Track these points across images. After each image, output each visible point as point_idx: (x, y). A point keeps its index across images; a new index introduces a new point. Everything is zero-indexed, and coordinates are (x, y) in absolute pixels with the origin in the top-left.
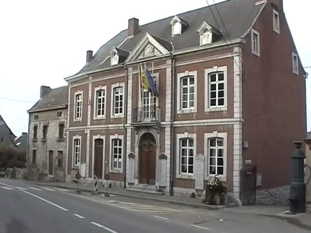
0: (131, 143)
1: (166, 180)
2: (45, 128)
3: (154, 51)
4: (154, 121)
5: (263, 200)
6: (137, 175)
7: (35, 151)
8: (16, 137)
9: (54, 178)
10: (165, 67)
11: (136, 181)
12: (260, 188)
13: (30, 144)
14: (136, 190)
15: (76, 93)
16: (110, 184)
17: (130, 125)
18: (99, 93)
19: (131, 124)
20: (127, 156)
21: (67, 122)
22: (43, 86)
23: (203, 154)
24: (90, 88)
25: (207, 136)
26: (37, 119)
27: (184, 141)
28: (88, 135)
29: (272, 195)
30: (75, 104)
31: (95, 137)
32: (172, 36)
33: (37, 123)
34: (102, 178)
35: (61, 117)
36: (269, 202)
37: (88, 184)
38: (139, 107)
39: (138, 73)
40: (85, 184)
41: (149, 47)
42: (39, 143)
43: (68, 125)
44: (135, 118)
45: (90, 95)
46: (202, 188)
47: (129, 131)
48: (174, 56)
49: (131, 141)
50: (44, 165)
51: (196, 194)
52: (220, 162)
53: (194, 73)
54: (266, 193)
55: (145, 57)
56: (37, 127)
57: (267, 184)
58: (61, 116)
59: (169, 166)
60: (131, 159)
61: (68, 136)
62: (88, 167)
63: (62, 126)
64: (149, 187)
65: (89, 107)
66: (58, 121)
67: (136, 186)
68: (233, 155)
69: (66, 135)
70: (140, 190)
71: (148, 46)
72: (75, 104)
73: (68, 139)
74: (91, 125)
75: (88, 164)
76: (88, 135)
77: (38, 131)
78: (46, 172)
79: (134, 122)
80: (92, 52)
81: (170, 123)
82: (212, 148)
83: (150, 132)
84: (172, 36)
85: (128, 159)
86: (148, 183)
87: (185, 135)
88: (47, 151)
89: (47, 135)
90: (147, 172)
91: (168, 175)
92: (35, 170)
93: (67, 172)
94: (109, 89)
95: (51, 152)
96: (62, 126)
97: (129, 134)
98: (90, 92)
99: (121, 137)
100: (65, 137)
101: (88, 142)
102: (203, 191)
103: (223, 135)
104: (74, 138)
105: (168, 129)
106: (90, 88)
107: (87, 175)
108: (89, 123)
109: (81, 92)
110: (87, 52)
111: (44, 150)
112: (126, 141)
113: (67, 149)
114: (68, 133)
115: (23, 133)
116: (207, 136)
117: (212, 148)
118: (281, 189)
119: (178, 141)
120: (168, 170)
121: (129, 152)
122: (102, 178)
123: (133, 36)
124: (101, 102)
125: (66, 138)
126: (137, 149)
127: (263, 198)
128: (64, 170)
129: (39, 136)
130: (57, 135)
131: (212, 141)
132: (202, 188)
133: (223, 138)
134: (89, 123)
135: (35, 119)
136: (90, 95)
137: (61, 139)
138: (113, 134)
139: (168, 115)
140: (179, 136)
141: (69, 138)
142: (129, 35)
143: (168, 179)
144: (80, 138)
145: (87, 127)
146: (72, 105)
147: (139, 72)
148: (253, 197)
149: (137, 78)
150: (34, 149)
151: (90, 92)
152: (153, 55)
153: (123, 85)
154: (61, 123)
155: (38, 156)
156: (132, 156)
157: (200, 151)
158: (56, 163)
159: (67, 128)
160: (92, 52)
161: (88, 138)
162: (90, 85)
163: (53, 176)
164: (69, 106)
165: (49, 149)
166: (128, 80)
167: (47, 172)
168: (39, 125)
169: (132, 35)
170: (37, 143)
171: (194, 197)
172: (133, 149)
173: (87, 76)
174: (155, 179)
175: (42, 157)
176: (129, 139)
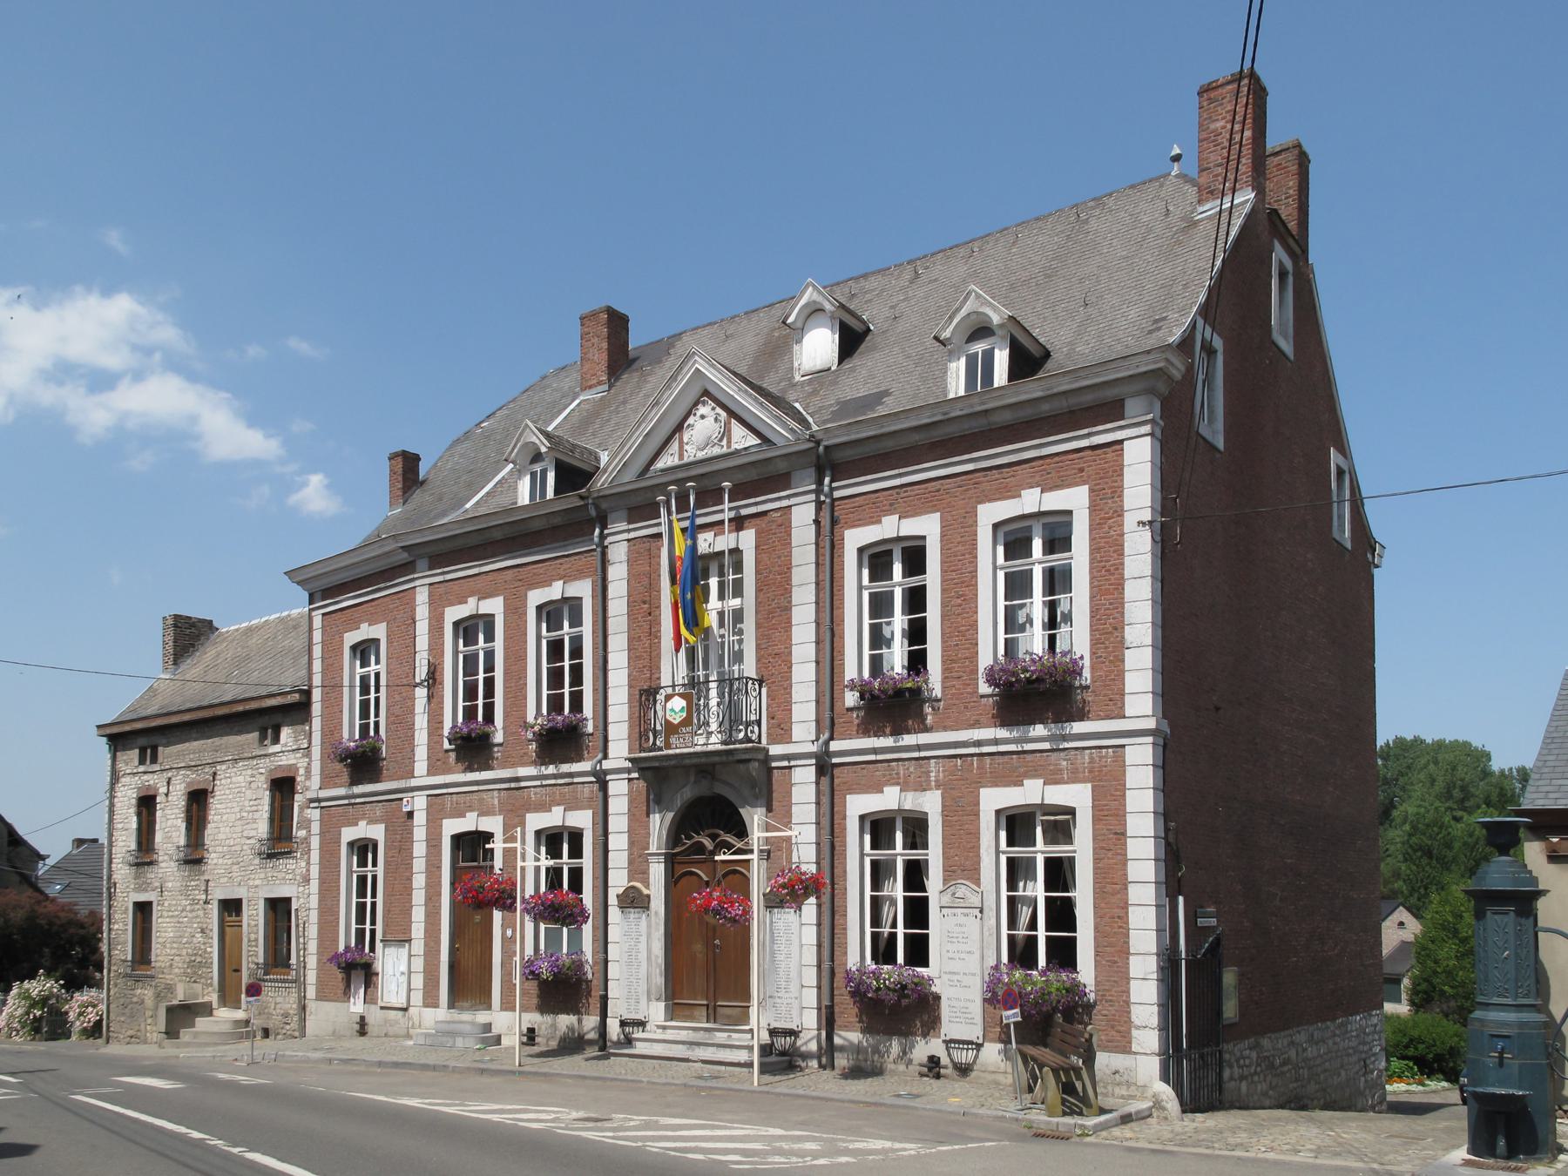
0: (631, 843)
1: (799, 998)
2: (198, 800)
3: (726, 433)
4: (741, 742)
5: (1244, 1086)
6: (659, 981)
7: (143, 910)
8: (43, 858)
9: (247, 1022)
10: (785, 503)
11: (656, 1012)
12: (1237, 1031)
13: (116, 877)
14: (658, 1050)
15: (352, 638)
16: (531, 1031)
17: (628, 764)
18: (468, 629)
19: (630, 760)
20: (613, 900)
21: (308, 770)
22: (177, 617)
23: (978, 882)
24: (422, 612)
25: (994, 799)
26: (154, 760)
27: (879, 828)
28: (420, 818)
29: (1272, 1066)
30: (346, 682)
31: (453, 826)
32: (798, 378)
33: (151, 780)
34: (489, 1007)
35: (277, 748)
36: (1265, 1094)
37: (427, 1035)
38: (665, 680)
39: (659, 535)
40: (408, 1036)
41: (703, 417)
42: (167, 866)
43: (316, 781)
44: (642, 727)
45: (422, 643)
46: (974, 1032)
47: (618, 788)
48: (826, 447)
49: (630, 831)
50: (195, 967)
51: (945, 1060)
52: (1061, 915)
53: (927, 526)
54: (1254, 1055)
55: (686, 460)
56: (153, 798)
57: (1258, 1022)
58: (276, 740)
59: (810, 936)
60: (633, 914)
61: (316, 828)
62: (418, 964)
63: (283, 787)
64: (721, 1037)
65: (421, 693)
66: (264, 766)
67: (659, 1035)
68: (1125, 884)
69: (306, 824)
70: (679, 1051)
71: (702, 410)
72: (346, 682)
73: (315, 843)
74: (430, 773)
75: (418, 946)
76: (420, 818)
77: (158, 814)
78: (206, 999)
79: (642, 750)
80: (417, 458)
81: (813, 748)
82: (1017, 851)
83: (721, 790)
84: (798, 378)
85: (614, 913)
86: (713, 1014)
87: (889, 799)
88: (206, 902)
89: (210, 830)
90: (708, 968)
91: (811, 977)
92: (147, 993)
93: (311, 992)
94: (515, 611)
95: (231, 907)
96: (283, 787)
97: (619, 805)
98: (422, 628)
99: (582, 819)
100: (302, 833)
101: (420, 849)
102: (979, 1046)
103: (1077, 796)
104: (349, 834)
105: (804, 775)
106: (422, 612)
107: (417, 998)
108: (421, 767)
109: (379, 631)
110: (392, 457)
111: (194, 902)
112: (606, 833)
113: (314, 886)
114: (315, 814)
115: (79, 842)
116: (994, 799)
117: (1017, 851)
118: (1301, 1037)
119: (852, 826)
120: (810, 957)
121: (619, 880)
122: (489, 1007)
123: (606, 387)
124: (368, 717)
125: (306, 840)
126: (657, 871)
127: (1242, 1078)
128: (300, 983)
129: (168, 838)
130: (262, 828)
131: (1017, 824)
132: (974, 1032)
133: (1071, 811)
134: (421, 767)
135: (142, 762)
136: (422, 643)
137: (280, 841)
138: (544, 807)
139: (804, 711)
140: (858, 805)
141: (322, 834)
142: (584, 389)
143: (811, 998)
144: (377, 832)
145: (414, 783)
146: (332, 687)
147: (664, 529)
148: (1212, 1077)
149: (653, 558)
150: (142, 897)
151: (422, 628)
152: (725, 450)
153: (583, 589)
154: (279, 775)
155: (164, 929)
156: (634, 901)
157: (963, 867)
158: (254, 950)
159: (310, 795)
160: (417, 458)
161: (420, 833)
162: (422, 596)
163: (240, 1015)
164: (317, 695)
165: (219, 894)
166: (604, 563)
167: (213, 998)
168: (163, 790)
169: (600, 383)
170: (151, 874)
171: (938, 1076)
172: (638, 868)
173: (404, 557)
174: (746, 995)
175: (183, 933)
176: (618, 823)
